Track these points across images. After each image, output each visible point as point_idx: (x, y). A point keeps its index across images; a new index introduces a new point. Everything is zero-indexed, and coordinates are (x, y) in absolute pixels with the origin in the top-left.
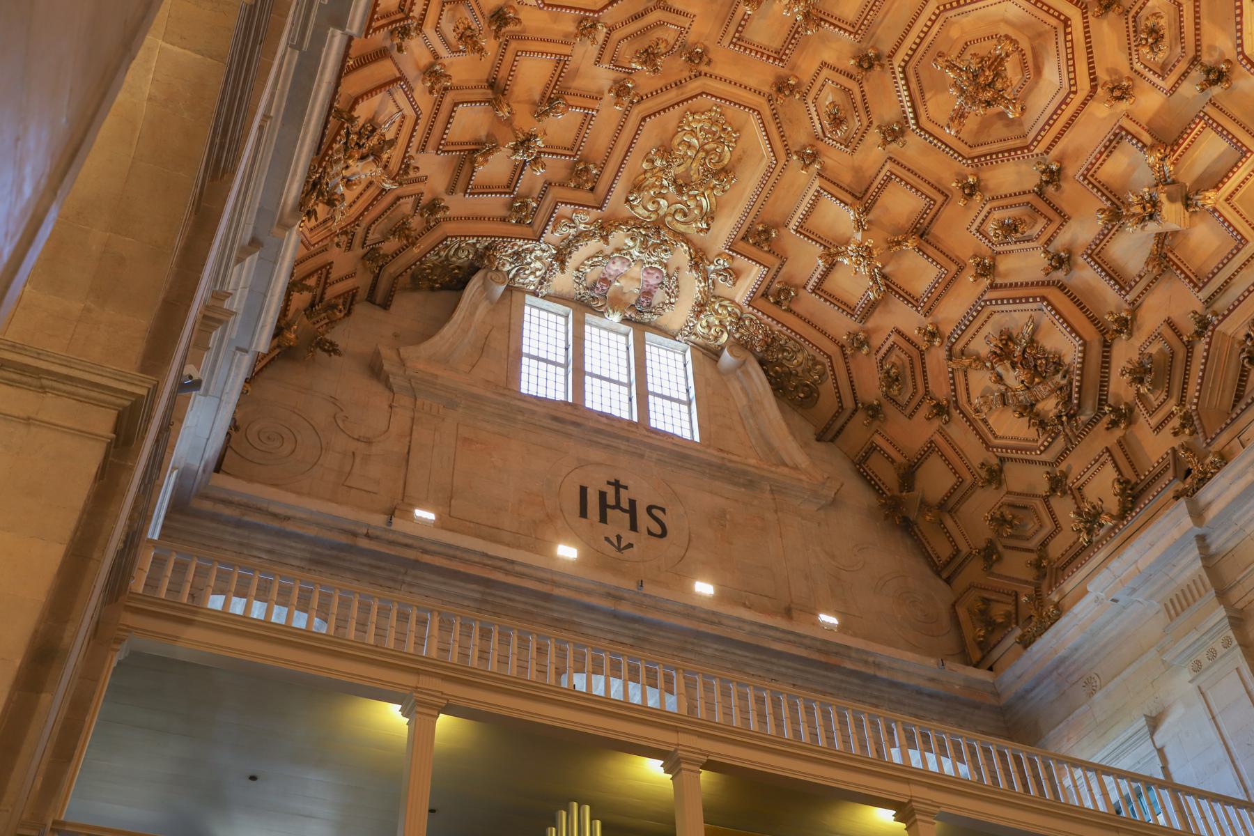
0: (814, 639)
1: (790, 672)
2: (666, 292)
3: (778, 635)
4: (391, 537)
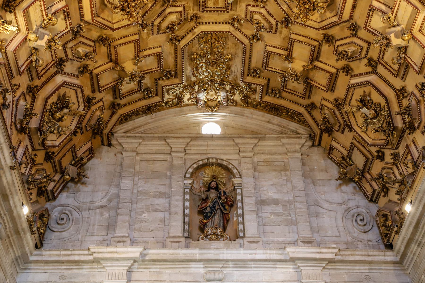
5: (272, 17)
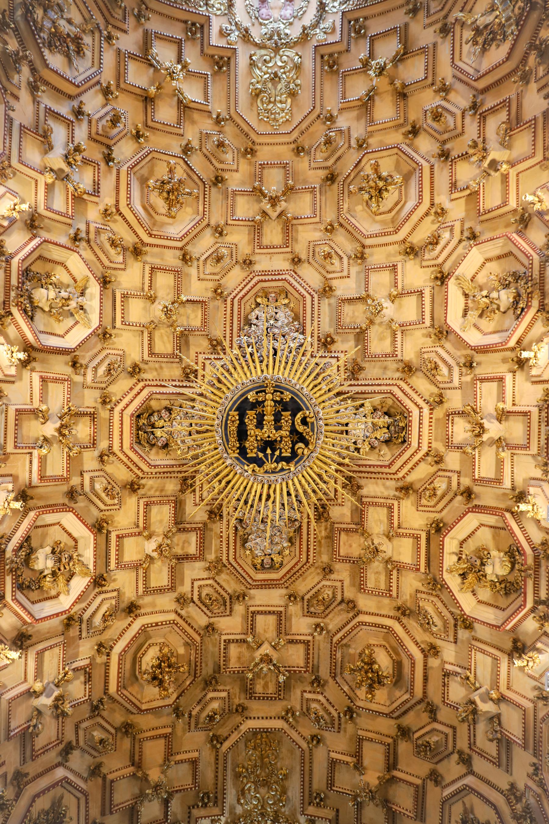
2: (252, 6)
5: (333, 706)
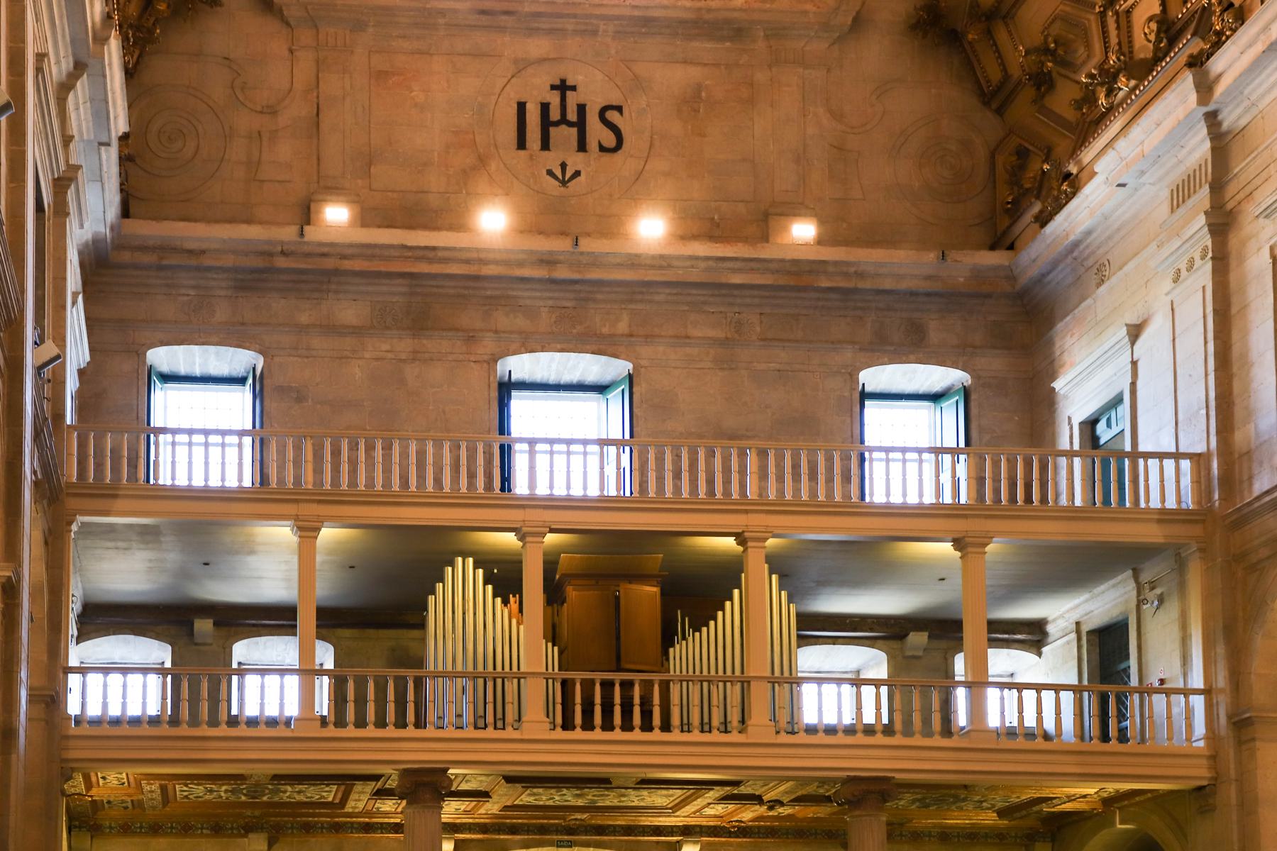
0: (782, 261)
1: (756, 301)
3: (738, 265)
4: (306, 249)
